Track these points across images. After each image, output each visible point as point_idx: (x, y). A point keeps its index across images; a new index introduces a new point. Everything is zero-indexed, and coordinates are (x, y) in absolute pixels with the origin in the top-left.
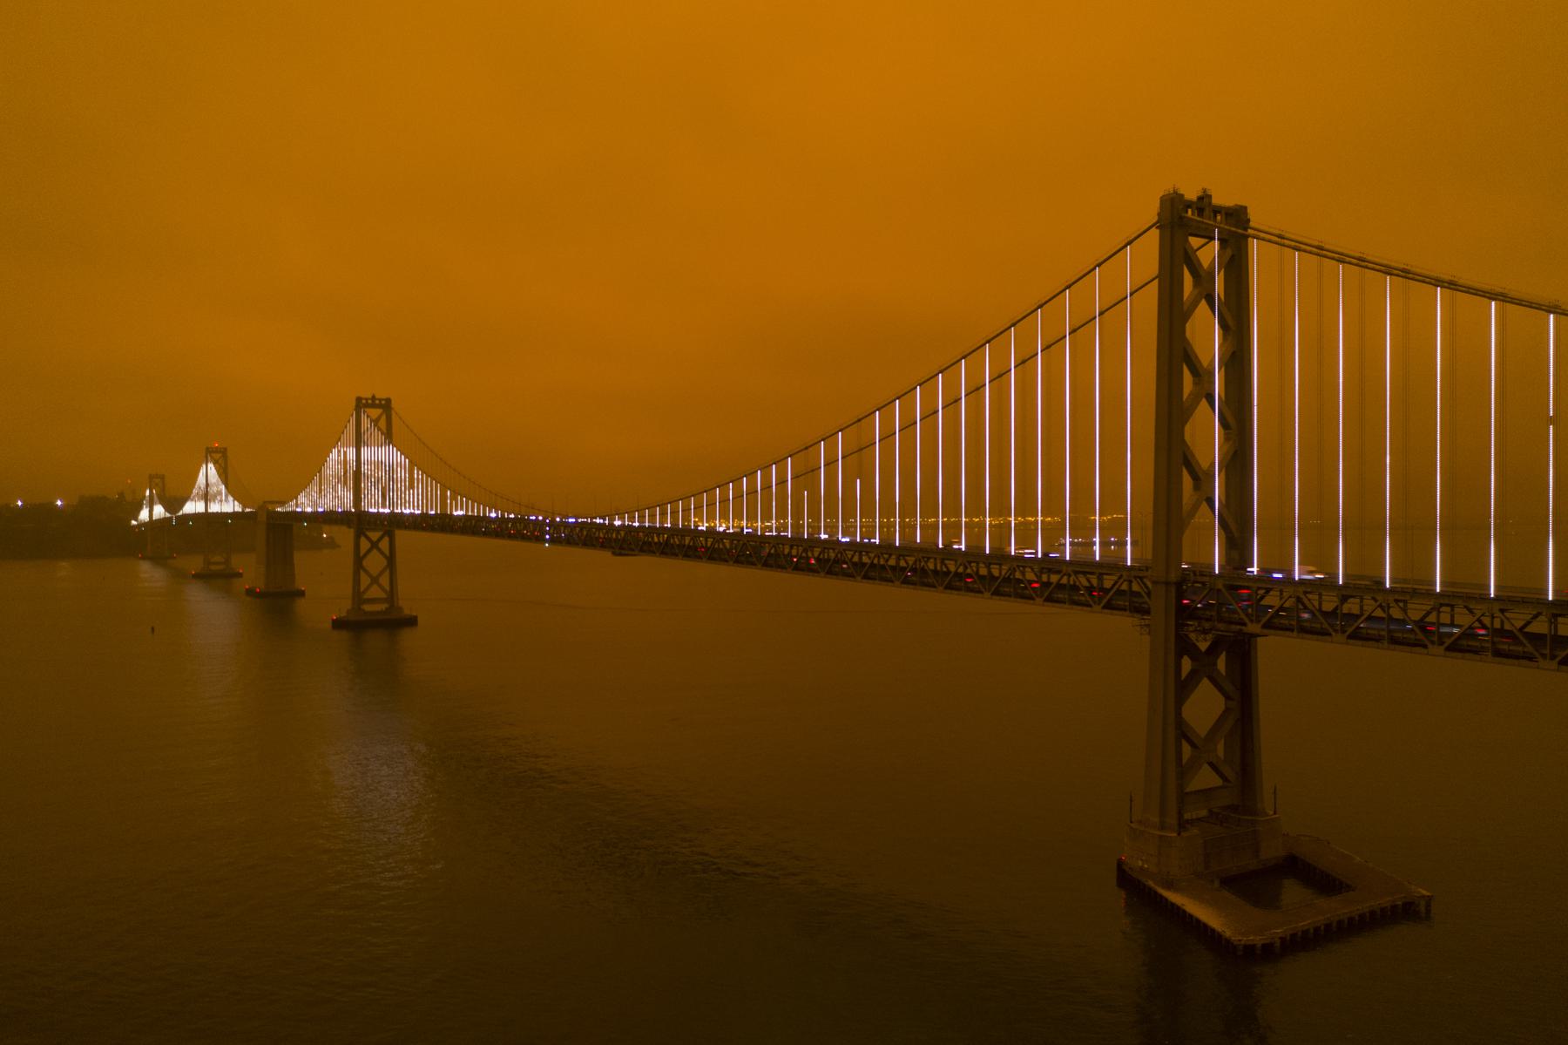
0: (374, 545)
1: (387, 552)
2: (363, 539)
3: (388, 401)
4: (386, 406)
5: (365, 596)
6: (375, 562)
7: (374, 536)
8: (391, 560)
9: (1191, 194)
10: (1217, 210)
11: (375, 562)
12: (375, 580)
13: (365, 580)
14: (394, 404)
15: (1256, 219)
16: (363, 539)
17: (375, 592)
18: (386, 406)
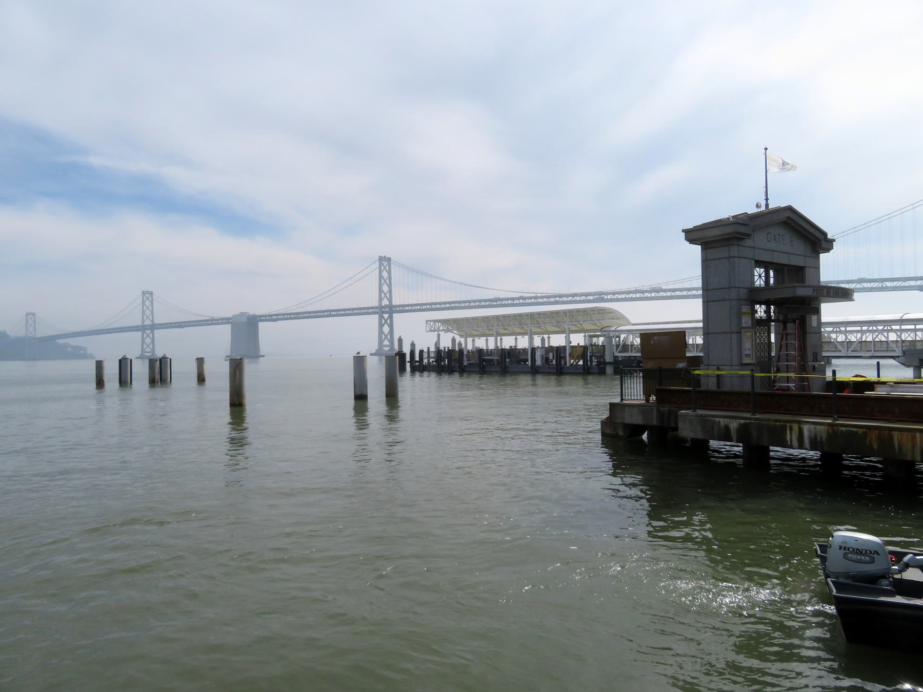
0: (148, 336)
1: (152, 337)
2: (145, 334)
3: (152, 292)
4: (151, 294)
5: (146, 351)
6: (148, 341)
7: (148, 332)
8: (153, 340)
9: (383, 256)
10: (387, 258)
11: (148, 341)
12: (148, 346)
13: (145, 346)
14: (154, 293)
15: (392, 259)
16: (145, 334)
17: (148, 350)
18: (151, 294)
